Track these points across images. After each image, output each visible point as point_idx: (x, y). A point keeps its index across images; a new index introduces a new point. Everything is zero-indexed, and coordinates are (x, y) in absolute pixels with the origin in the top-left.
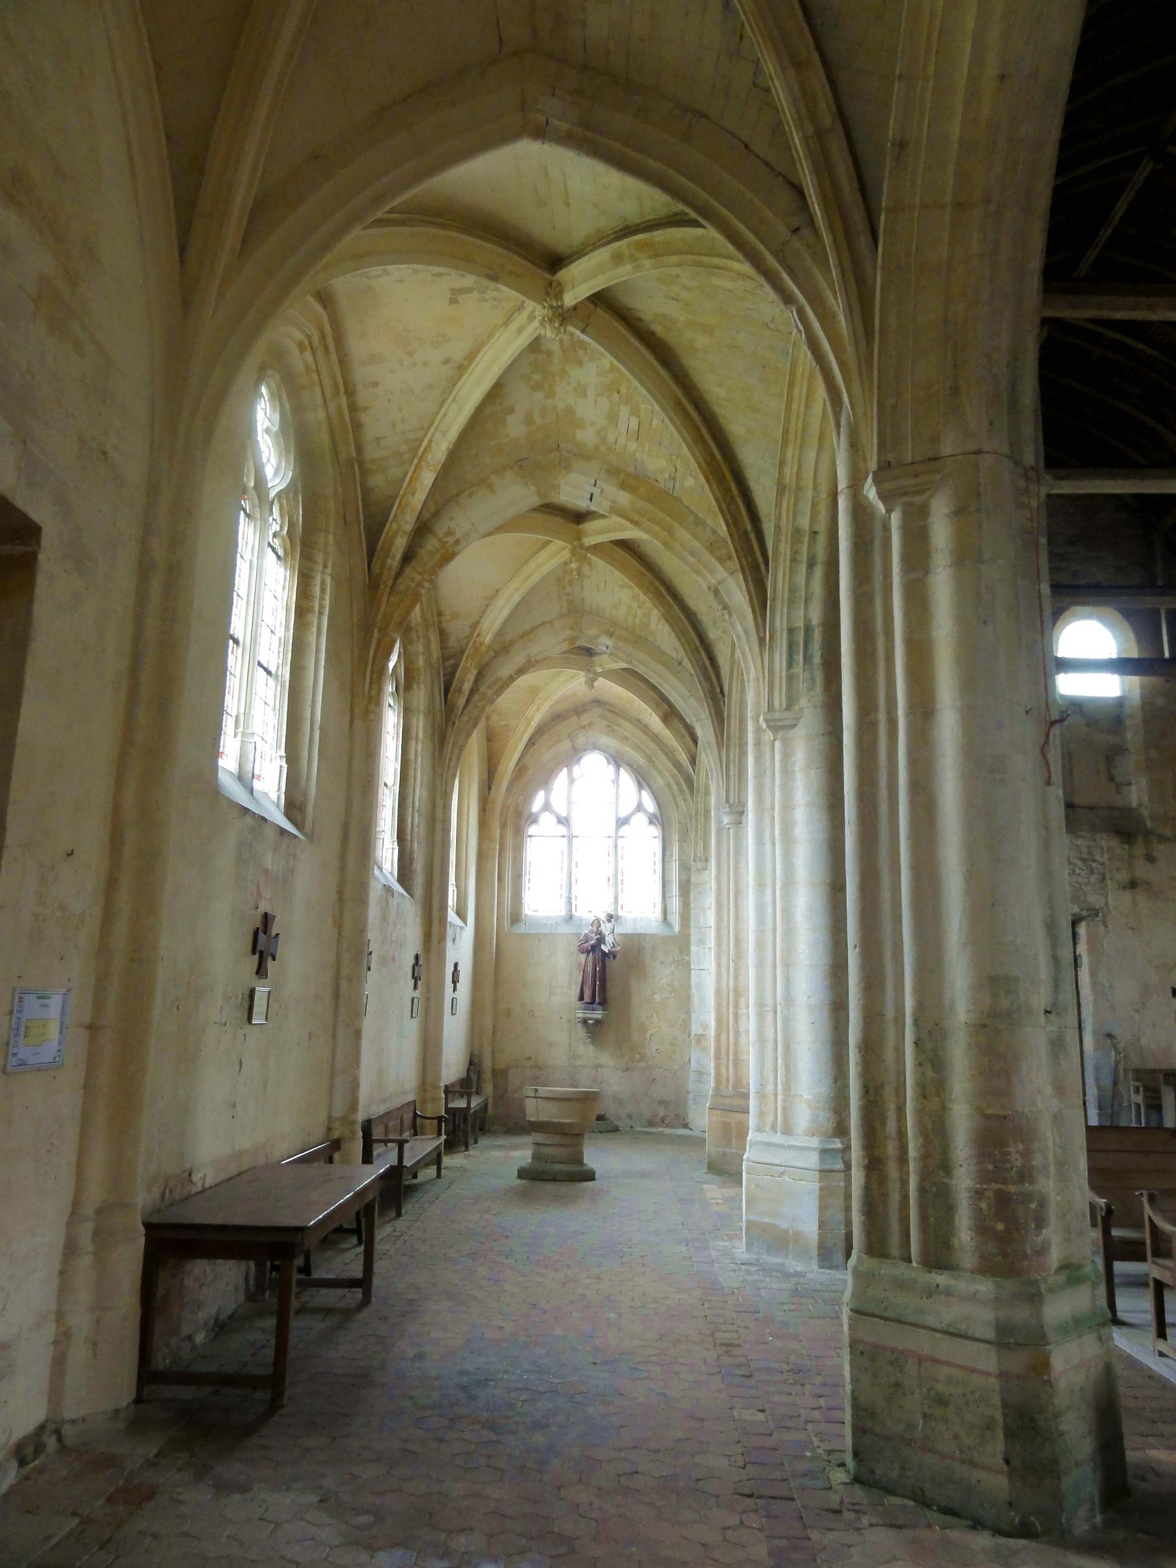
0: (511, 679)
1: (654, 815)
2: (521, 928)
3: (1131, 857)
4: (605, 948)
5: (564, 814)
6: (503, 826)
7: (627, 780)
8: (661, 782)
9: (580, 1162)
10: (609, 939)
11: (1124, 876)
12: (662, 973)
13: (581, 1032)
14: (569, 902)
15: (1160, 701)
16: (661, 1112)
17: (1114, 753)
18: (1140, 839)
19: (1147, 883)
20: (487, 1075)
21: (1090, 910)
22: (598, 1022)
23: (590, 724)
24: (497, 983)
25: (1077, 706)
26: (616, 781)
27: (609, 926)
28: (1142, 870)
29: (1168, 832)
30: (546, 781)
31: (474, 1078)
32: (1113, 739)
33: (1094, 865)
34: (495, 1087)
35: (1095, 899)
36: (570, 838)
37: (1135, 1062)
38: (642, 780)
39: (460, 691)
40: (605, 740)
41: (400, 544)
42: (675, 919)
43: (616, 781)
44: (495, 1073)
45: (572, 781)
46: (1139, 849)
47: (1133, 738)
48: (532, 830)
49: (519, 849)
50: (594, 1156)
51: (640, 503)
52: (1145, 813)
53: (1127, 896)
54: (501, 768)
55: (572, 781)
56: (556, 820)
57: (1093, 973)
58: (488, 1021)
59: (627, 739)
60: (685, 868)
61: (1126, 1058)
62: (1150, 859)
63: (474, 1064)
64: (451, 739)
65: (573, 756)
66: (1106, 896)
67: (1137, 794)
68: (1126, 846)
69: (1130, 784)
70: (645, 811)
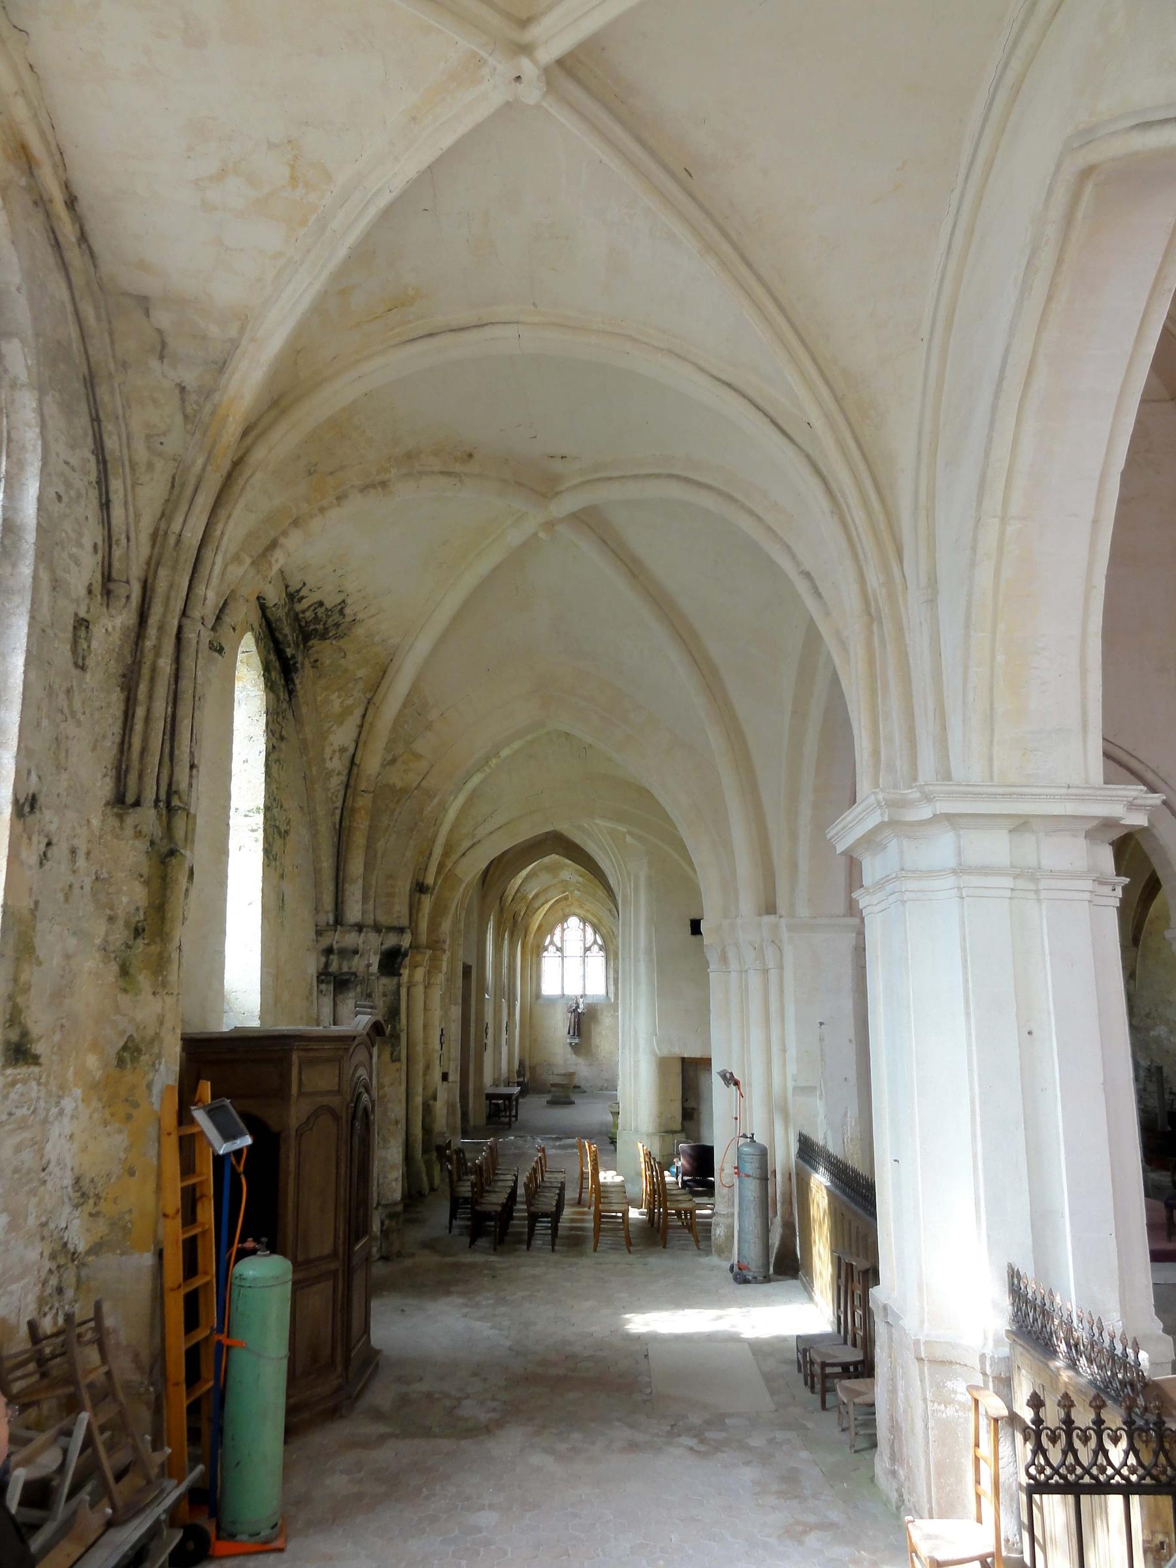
0: (539, 908)
1: (601, 946)
2: (541, 1001)
4: (579, 1011)
5: (559, 946)
6: (532, 953)
7: (589, 930)
8: (605, 931)
9: (568, 1097)
10: (581, 1006)
12: (606, 1020)
13: (569, 1049)
14: (563, 988)
16: (606, 1085)
20: (527, 1069)
22: (576, 1044)
23: (572, 904)
24: (531, 1026)
26: (584, 930)
27: (581, 1000)
30: (551, 932)
31: (521, 1069)
34: (531, 1074)
36: (563, 957)
38: (596, 929)
39: (519, 915)
40: (578, 911)
41: (510, 898)
42: (612, 996)
43: (584, 930)
44: (530, 1067)
45: (563, 930)
48: (545, 954)
49: (539, 964)
50: (574, 1098)
51: (585, 881)
54: (530, 928)
55: (563, 930)
56: (555, 949)
58: (527, 1045)
59: (589, 911)
60: (616, 971)
63: (521, 1063)
64: (515, 933)
65: (565, 918)
70: (598, 944)
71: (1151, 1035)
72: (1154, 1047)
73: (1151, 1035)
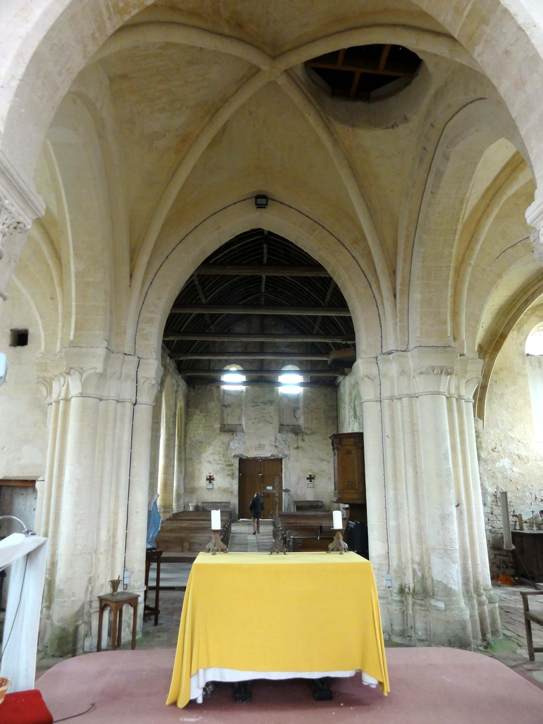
3: (298, 440)
11: (295, 446)
15: (309, 394)
17: (295, 410)
18: (300, 435)
19: (301, 447)
21: (285, 455)
25: (285, 396)
28: (301, 443)
29: (309, 432)
32: (296, 405)
33: (287, 442)
35: (286, 452)
37: (295, 499)
46: (300, 437)
47: (301, 405)
52: (303, 427)
53: (296, 451)
57: (285, 473)
61: (292, 497)
62: (303, 440)
66: (290, 452)
67: (301, 422)
68: (296, 437)
69: (300, 418)
71: (497, 466)
72: (499, 476)
73: (497, 466)
